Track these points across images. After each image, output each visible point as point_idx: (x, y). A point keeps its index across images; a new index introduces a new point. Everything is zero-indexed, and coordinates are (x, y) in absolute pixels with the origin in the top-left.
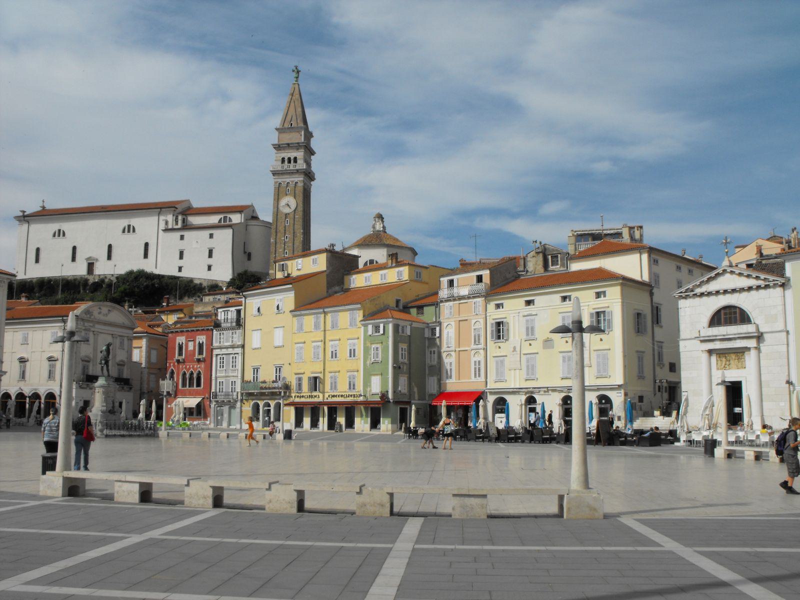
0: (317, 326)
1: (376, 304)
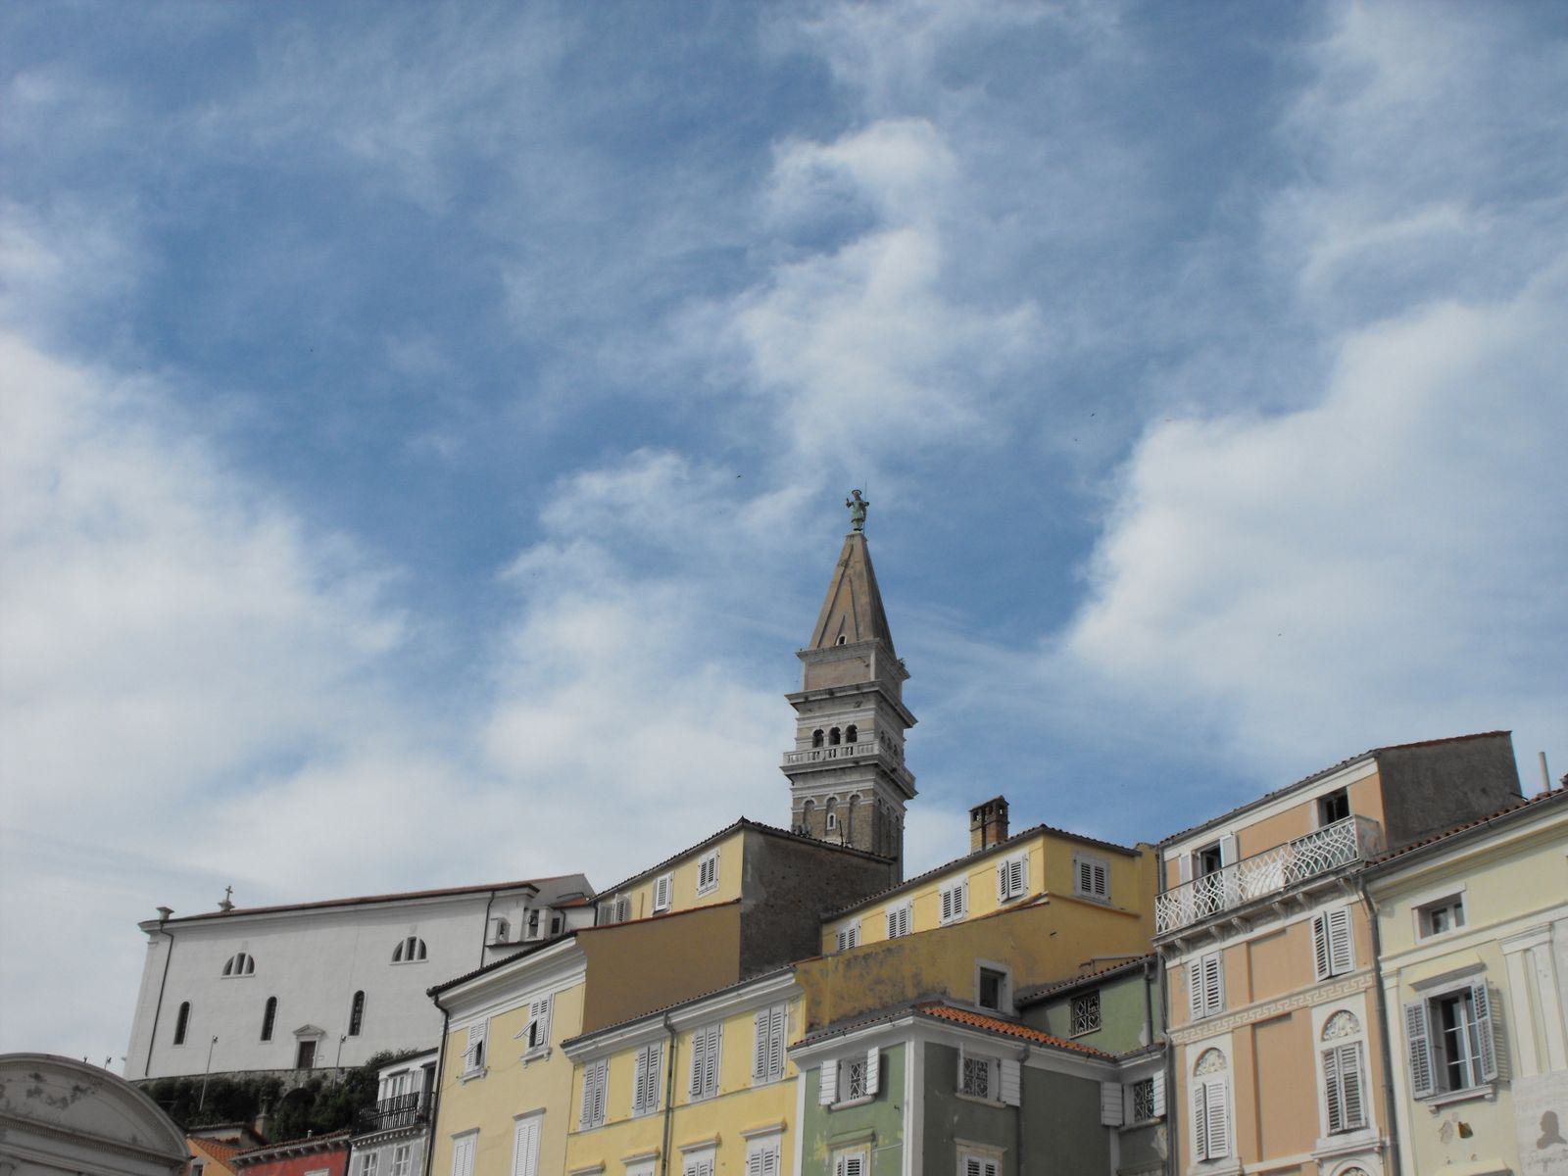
0: (645, 1097)
1: (879, 981)
